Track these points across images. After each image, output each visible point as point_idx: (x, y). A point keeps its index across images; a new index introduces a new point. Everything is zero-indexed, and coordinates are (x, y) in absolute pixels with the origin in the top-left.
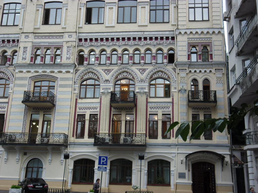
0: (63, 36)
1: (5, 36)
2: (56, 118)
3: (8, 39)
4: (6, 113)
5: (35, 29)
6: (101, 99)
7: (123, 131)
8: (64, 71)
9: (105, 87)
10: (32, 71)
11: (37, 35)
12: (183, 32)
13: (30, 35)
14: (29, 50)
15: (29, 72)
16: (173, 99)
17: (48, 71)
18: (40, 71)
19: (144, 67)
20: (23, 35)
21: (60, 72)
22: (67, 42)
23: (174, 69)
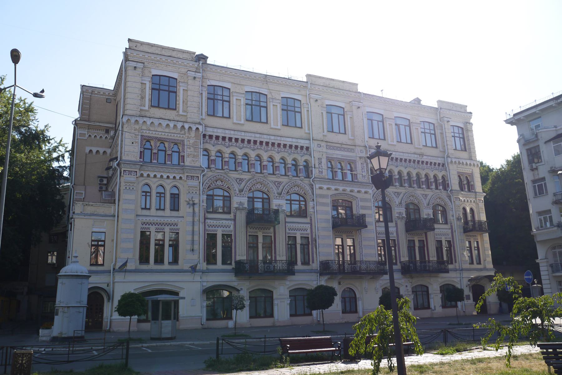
0: (353, 149)
1: (294, 140)
2: (364, 243)
3: (297, 144)
4: (310, 236)
5: (324, 136)
6: (396, 224)
7: (418, 258)
8: (363, 190)
9: (399, 211)
10: (333, 188)
11: (328, 144)
12: (454, 160)
13: (323, 144)
14: (324, 161)
15: (328, 189)
16: (452, 226)
17: (348, 189)
19: (426, 193)
20: (316, 143)
21: (359, 192)
22: (360, 158)
23: (449, 197)
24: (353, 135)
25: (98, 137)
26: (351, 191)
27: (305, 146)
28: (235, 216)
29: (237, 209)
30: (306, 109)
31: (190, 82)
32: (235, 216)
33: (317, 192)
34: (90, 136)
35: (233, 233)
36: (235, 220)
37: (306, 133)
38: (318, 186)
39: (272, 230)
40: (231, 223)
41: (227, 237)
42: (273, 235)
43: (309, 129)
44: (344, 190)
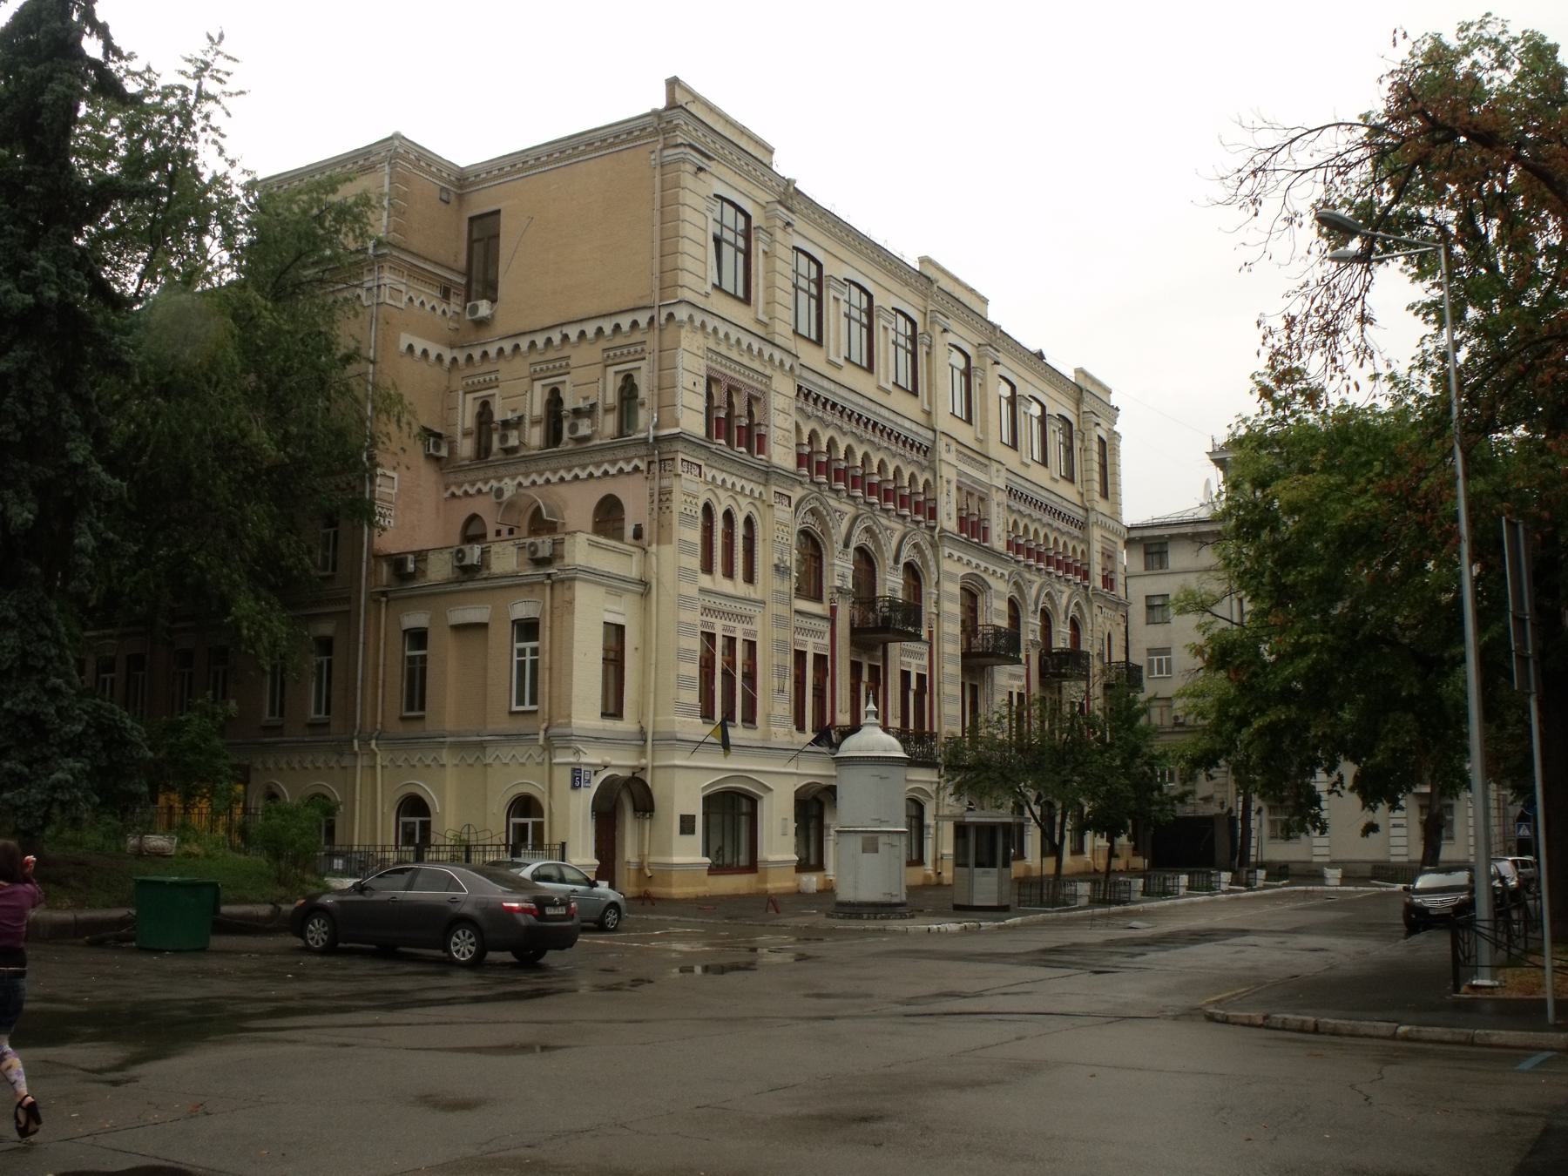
13: (954, 446)
17: (983, 565)
18: (974, 561)
24: (985, 430)
25: (428, 307)
26: (986, 569)
27: (926, 443)
28: (833, 610)
29: (839, 590)
30: (925, 349)
31: (779, 235)
32: (833, 610)
33: (947, 565)
34: (411, 299)
35: (828, 653)
36: (832, 619)
37: (924, 411)
38: (947, 551)
39: (880, 653)
40: (825, 626)
41: (820, 659)
42: (880, 664)
43: (930, 403)
44: (978, 566)
